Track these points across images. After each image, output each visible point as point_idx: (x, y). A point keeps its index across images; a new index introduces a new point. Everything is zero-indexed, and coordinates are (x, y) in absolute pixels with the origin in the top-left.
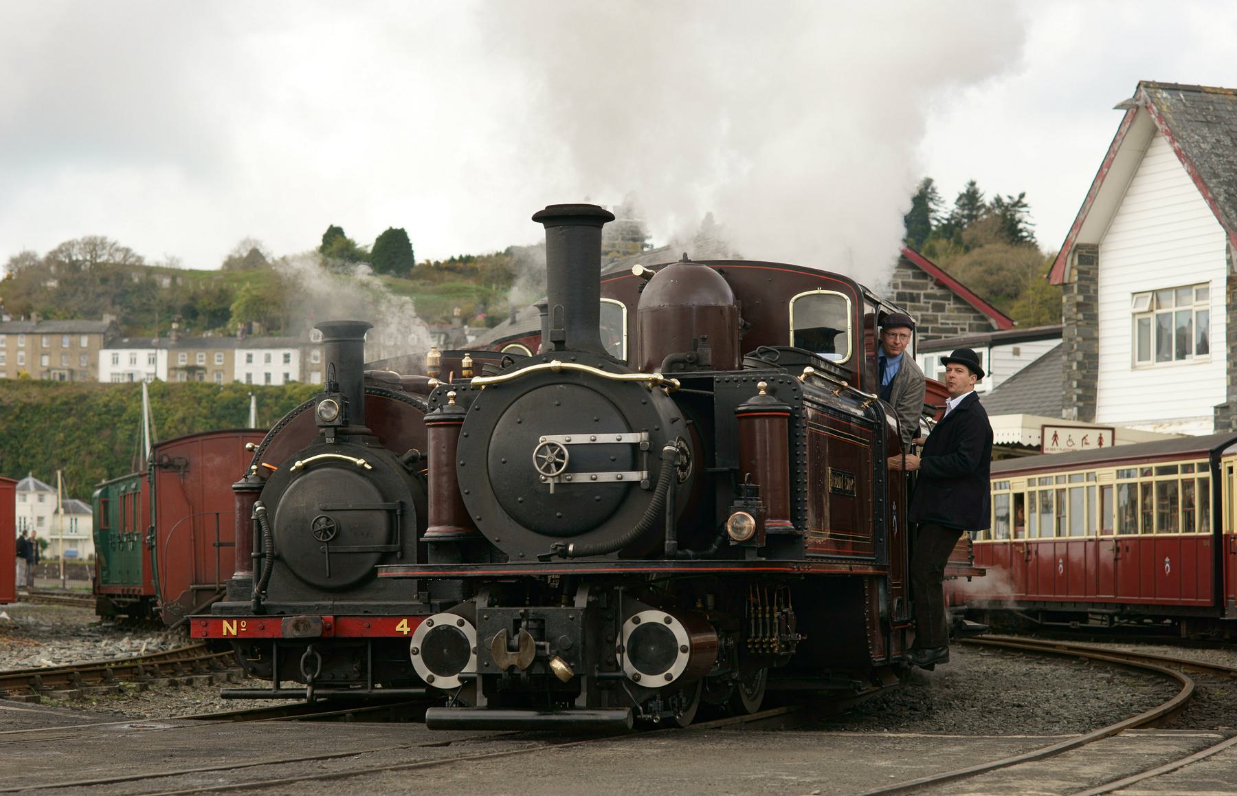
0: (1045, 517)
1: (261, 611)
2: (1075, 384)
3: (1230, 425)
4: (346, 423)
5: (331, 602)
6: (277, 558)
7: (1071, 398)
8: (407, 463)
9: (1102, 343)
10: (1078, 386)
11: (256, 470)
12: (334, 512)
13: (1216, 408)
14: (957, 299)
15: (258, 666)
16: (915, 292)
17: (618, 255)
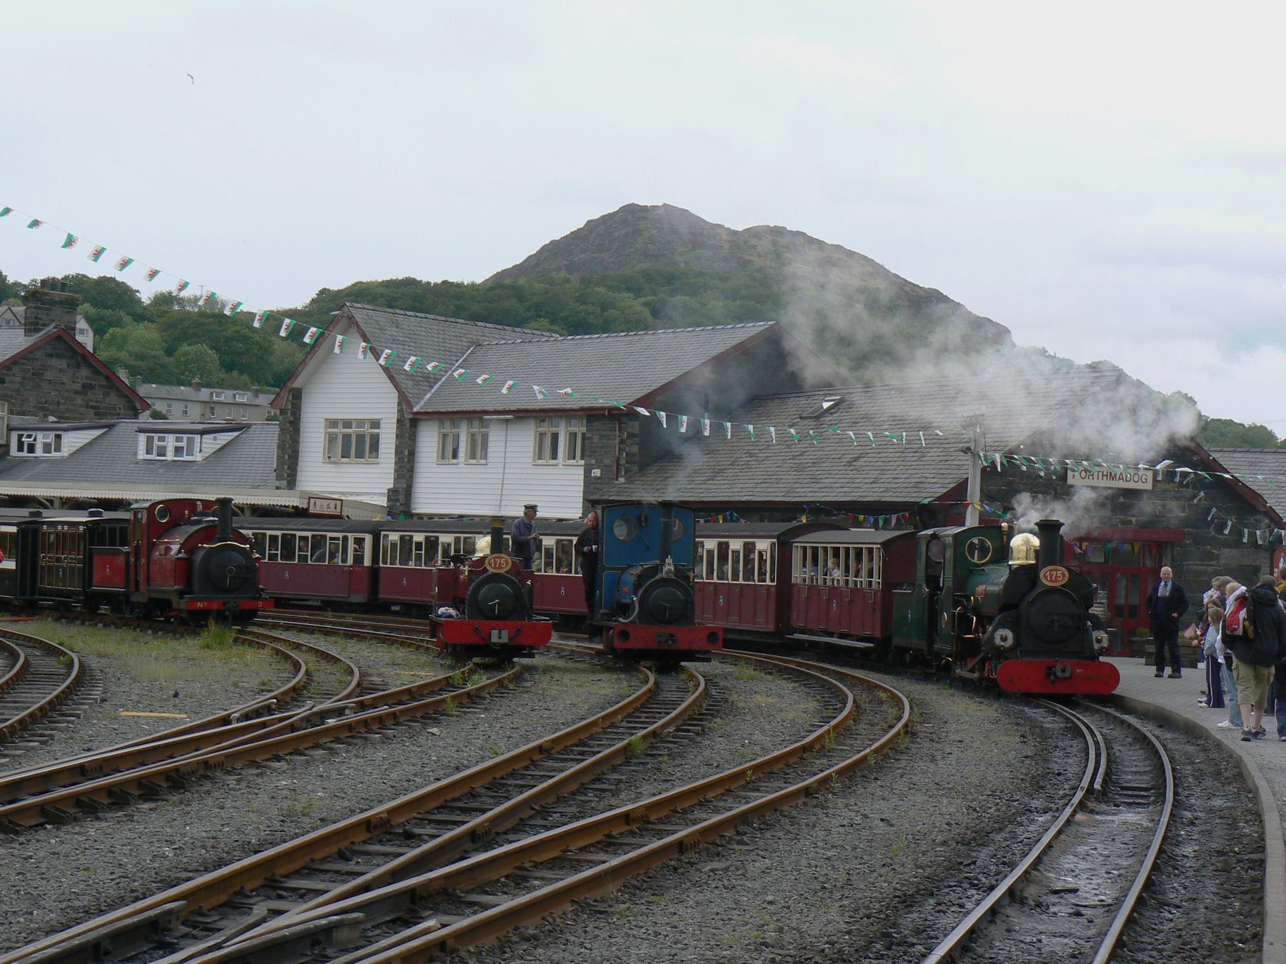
0: (44, 515)
2: (286, 467)
3: (398, 500)
7: (283, 475)
9: (301, 444)
10: (288, 469)
13: (389, 490)
14: (117, 389)
16: (93, 383)
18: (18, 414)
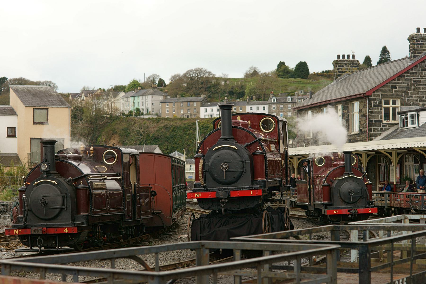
1: (26, 227)
4: (49, 171)
5: (46, 223)
6: (31, 211)
8: (68, 182)
11: (25, 185)
12: (47, 197)
15: (25, 242)
17: (349, 72)
18: (406, 105)
